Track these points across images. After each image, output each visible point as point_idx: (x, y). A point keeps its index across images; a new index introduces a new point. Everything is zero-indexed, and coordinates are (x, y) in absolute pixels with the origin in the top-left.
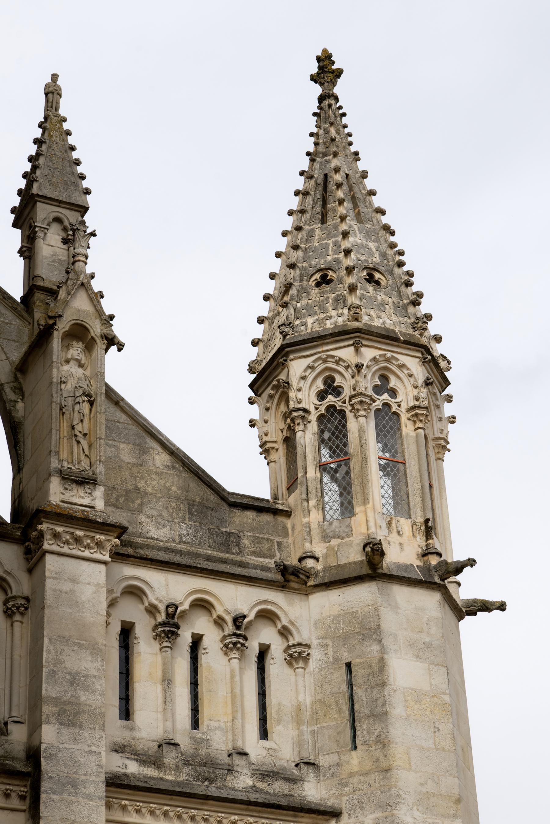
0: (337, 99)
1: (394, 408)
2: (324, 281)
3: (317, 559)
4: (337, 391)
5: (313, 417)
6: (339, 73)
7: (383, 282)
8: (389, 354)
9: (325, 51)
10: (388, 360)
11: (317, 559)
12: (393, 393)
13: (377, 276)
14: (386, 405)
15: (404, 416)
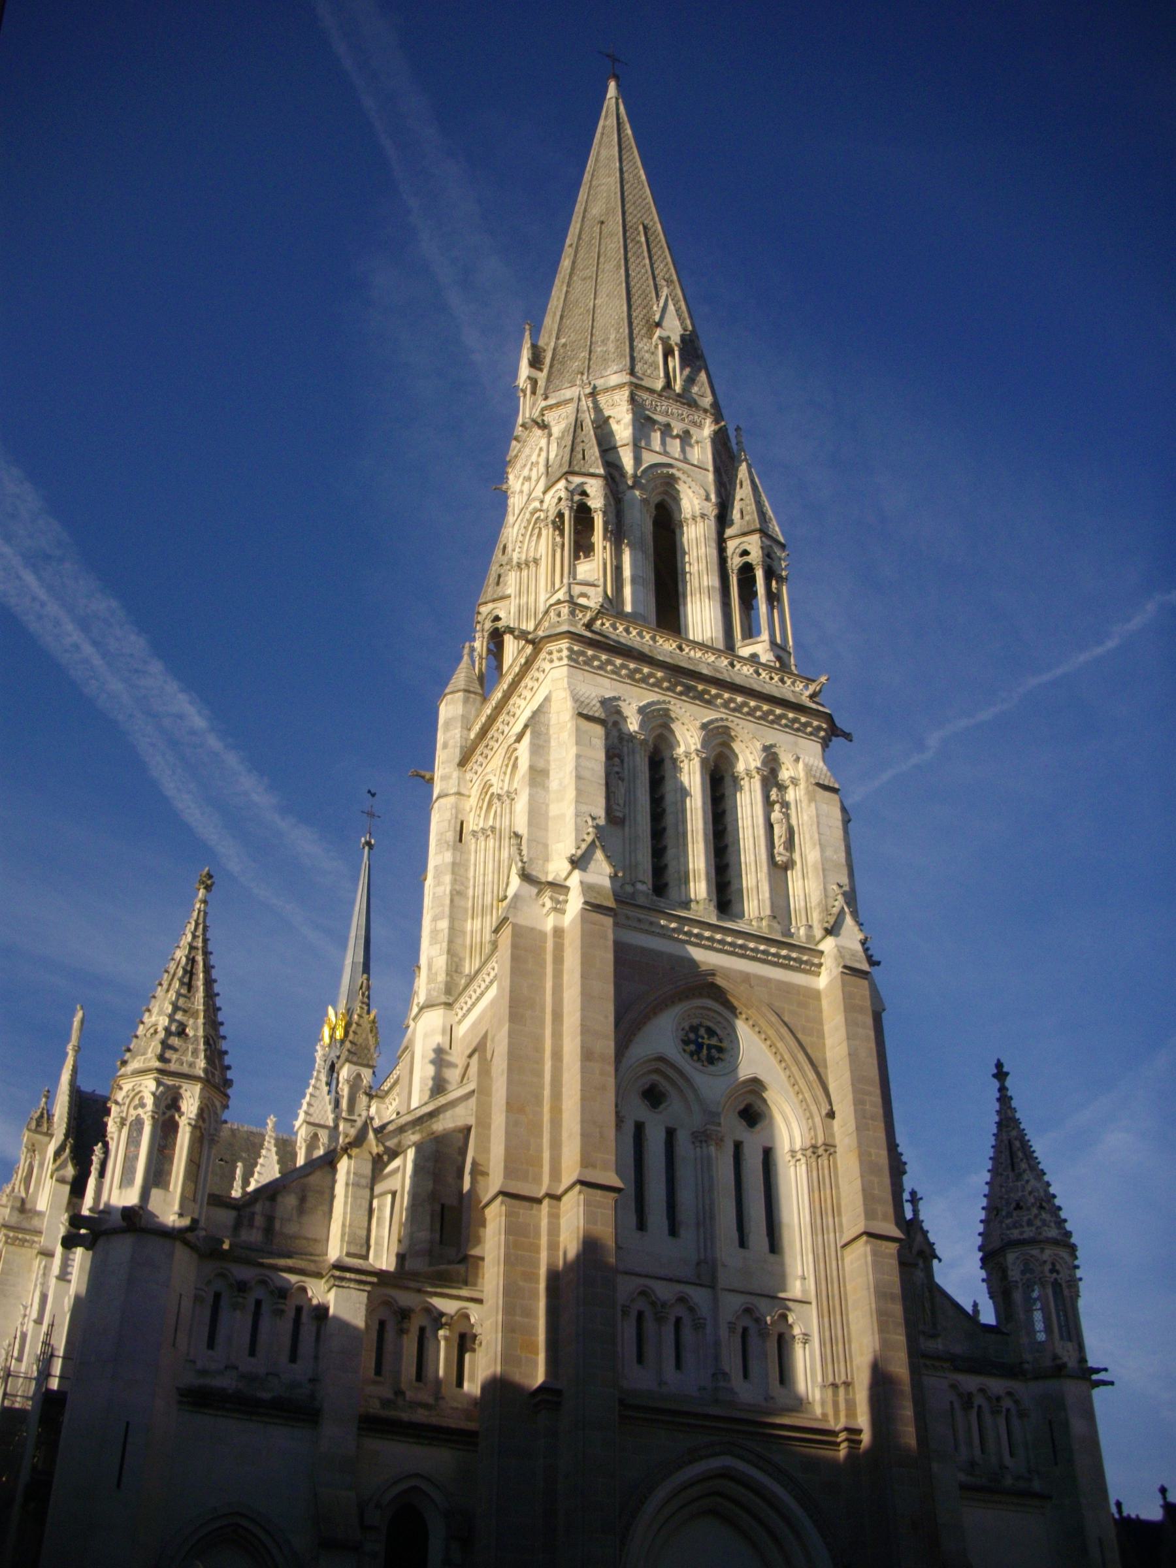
0: (1007, 1089)
1: (1059, 1281)
2: (1018, 1207)
3: (1028, 1363)
4: (1032, 1271)
5: (1020, 1285)
6: (1007, 1074)
7: (1047, 1207)
8: (1056, 1252)
9: (999, 1060)
10: (1055, 1255)
11: (1028, 1363)
12: (1058, 1272)
13: (1044, 1204)
14: (1056, 1279)
15: (1064, 1285)
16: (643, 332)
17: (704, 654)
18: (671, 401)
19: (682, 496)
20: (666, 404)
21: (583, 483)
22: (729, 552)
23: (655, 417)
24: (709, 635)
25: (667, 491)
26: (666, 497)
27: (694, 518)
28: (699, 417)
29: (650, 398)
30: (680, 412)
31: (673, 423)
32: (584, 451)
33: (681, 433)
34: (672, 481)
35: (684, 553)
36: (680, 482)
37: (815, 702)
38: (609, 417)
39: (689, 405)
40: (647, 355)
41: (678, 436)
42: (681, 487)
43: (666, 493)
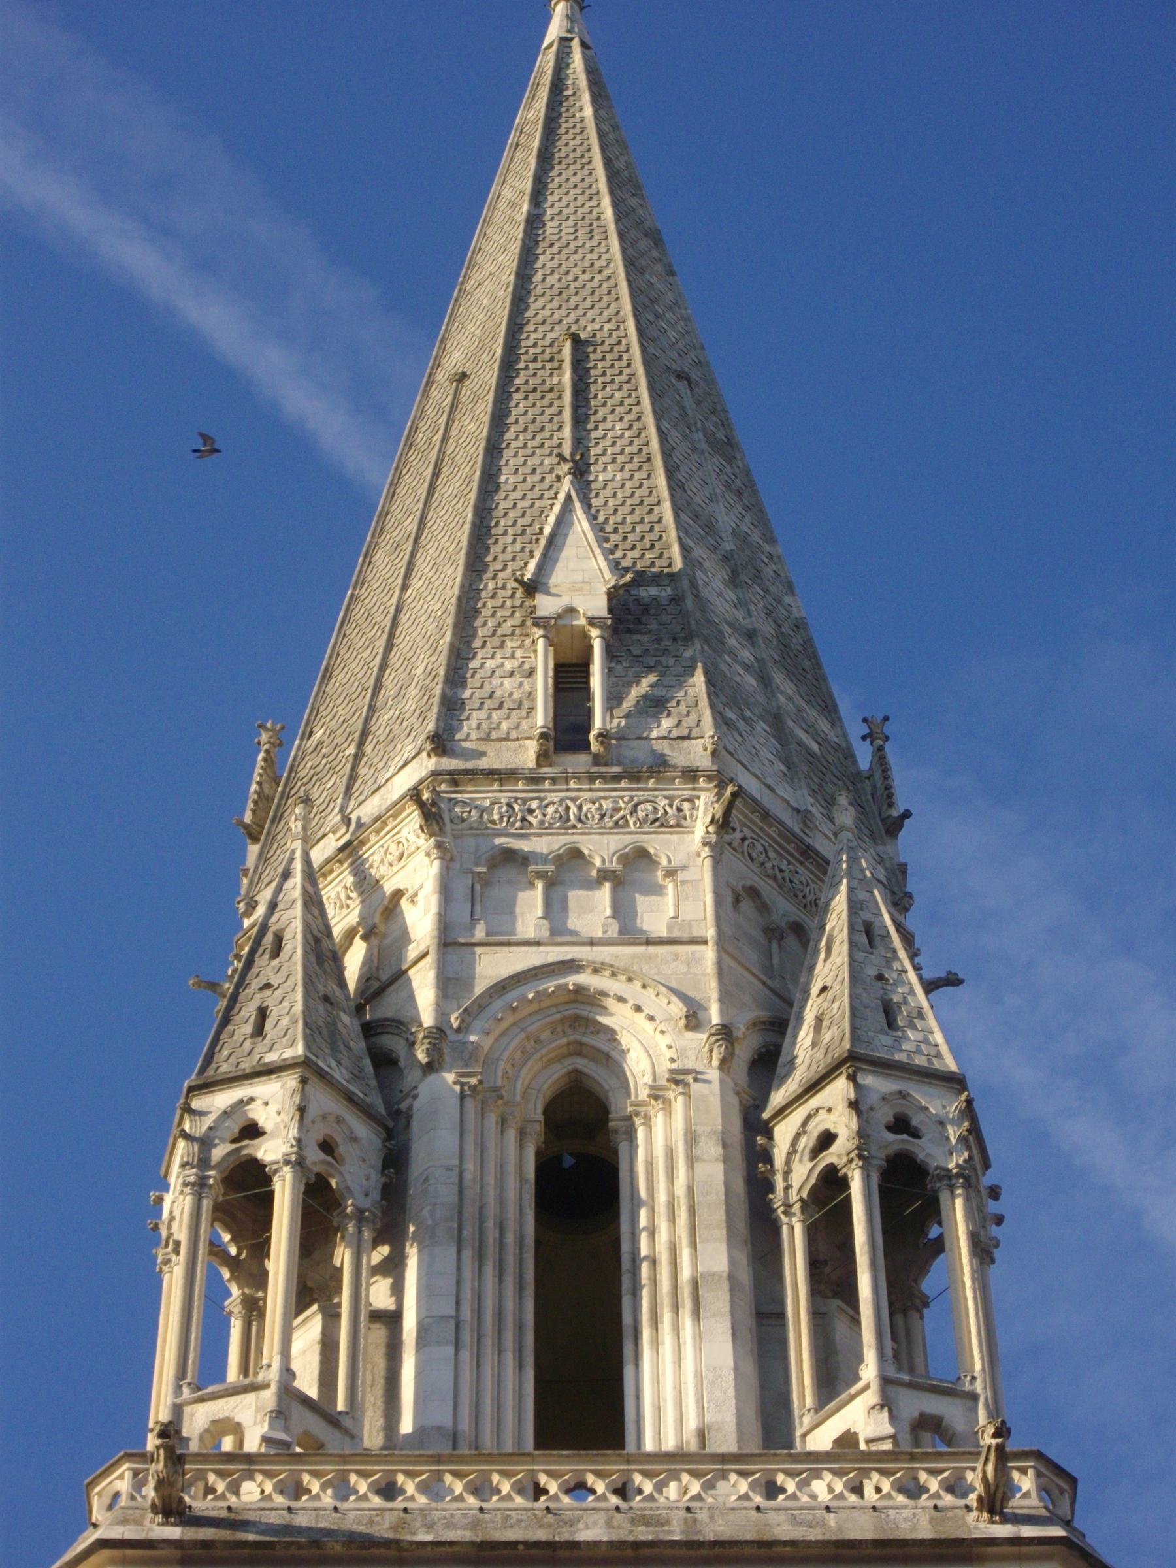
16: (507, 628)
17: (709, 1486)
18: (572, 785)
19: (625, 1040)
20: (555, 797)
21: (242, 1103)
22: (779, 1155)
23: (524, 846)
24: (692, 1423)
25: (580, 1044)
26: (582, 1064)
27: (656, 1094)
28: (671, 799)
29: (504, 798)
30: (607, 805)
31: (587, 844)
32: (263, 1013)
33: (614, 865)
34: (583, 1011)
35: (636, 1203)
36: (611, 1003)
37: (1006, 1519)
38: (398, 894)
39: (634, 776)
40: (508, 683)
41: (605, 875)
42: (617, 1018)
43: (578, 1049)
